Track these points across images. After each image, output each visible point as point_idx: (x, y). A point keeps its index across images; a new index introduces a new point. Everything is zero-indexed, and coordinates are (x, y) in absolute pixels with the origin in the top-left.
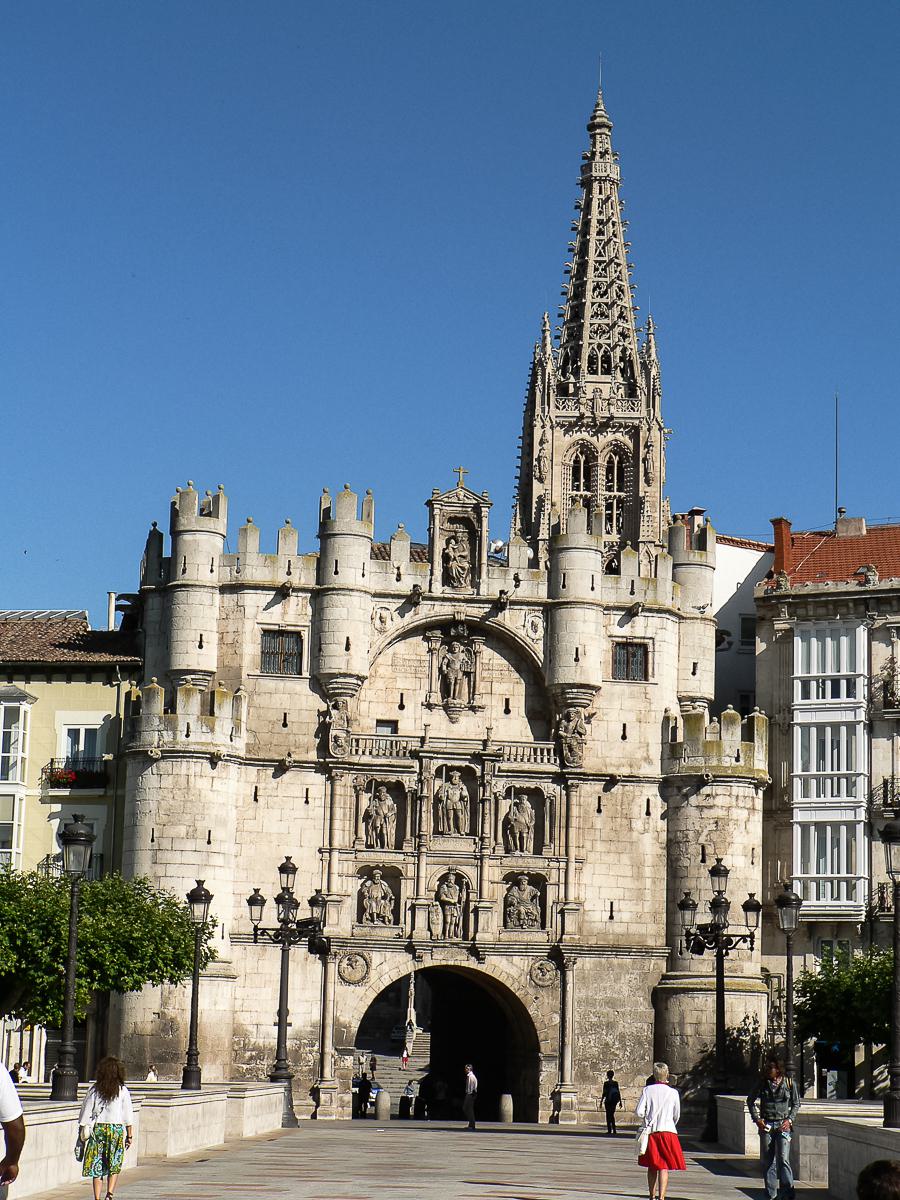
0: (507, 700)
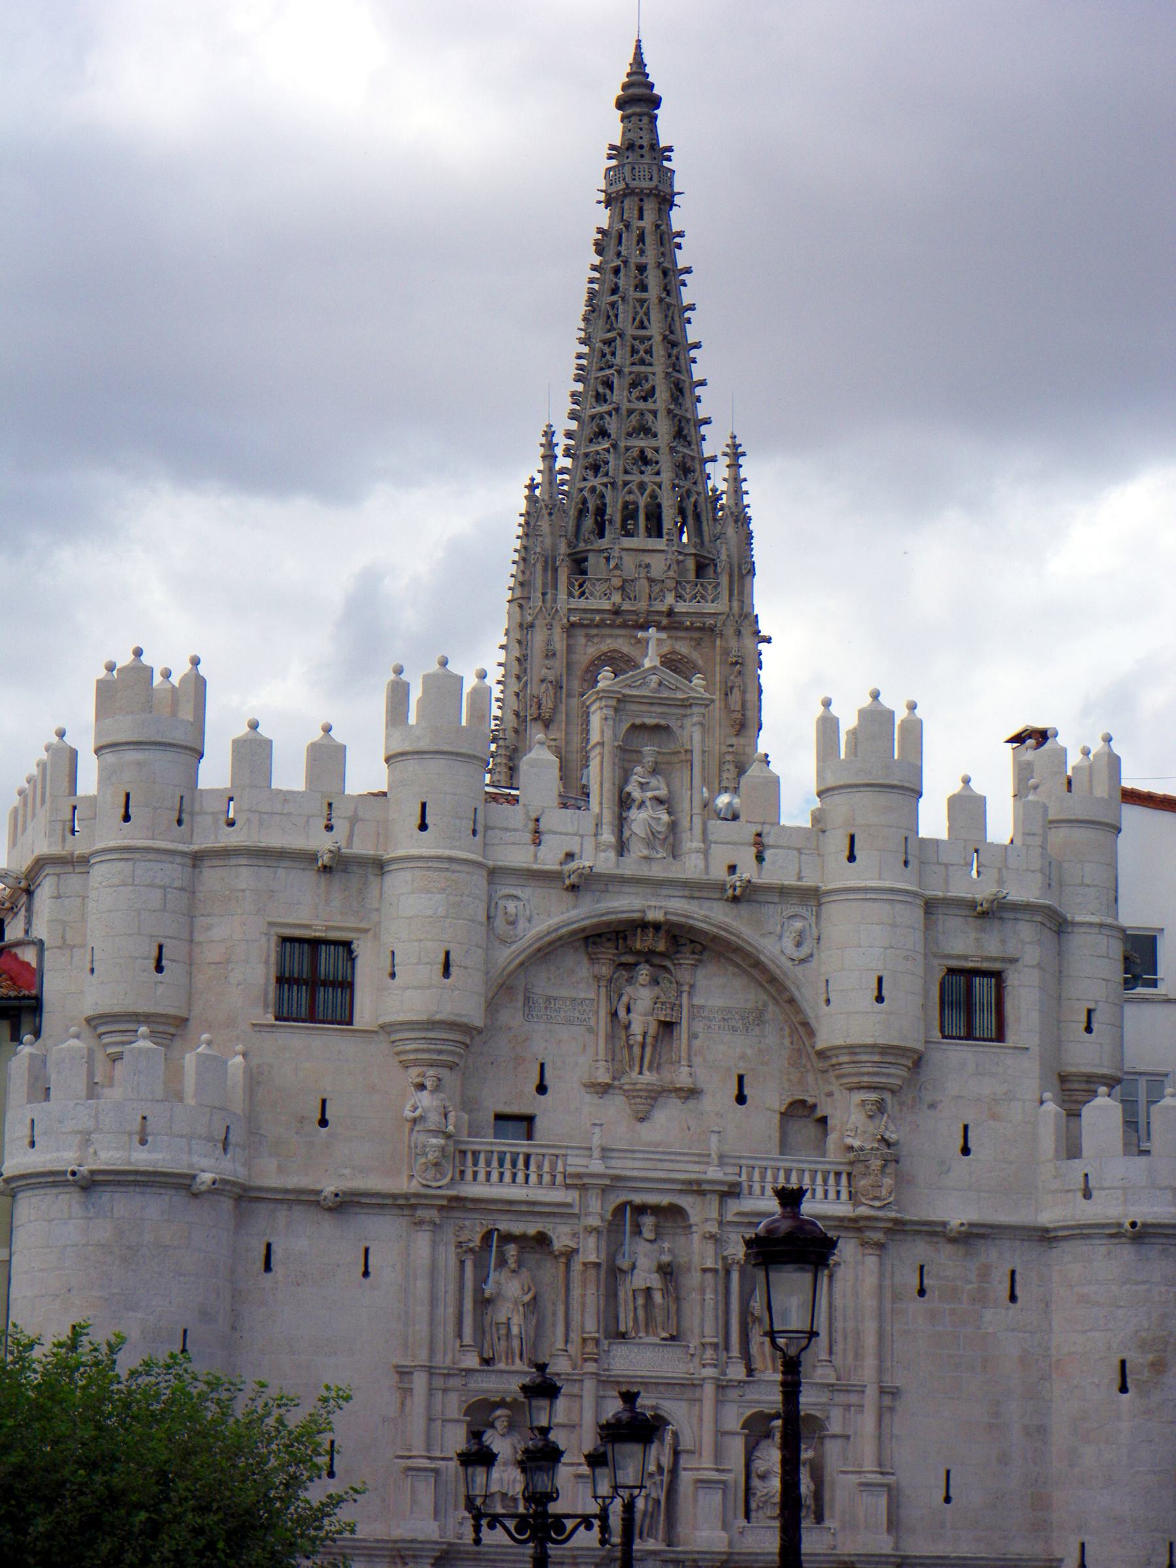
0: (741, 1078)
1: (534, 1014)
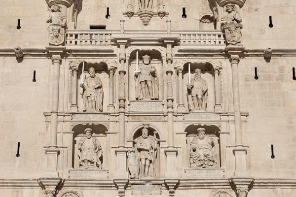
0: (184, 9)
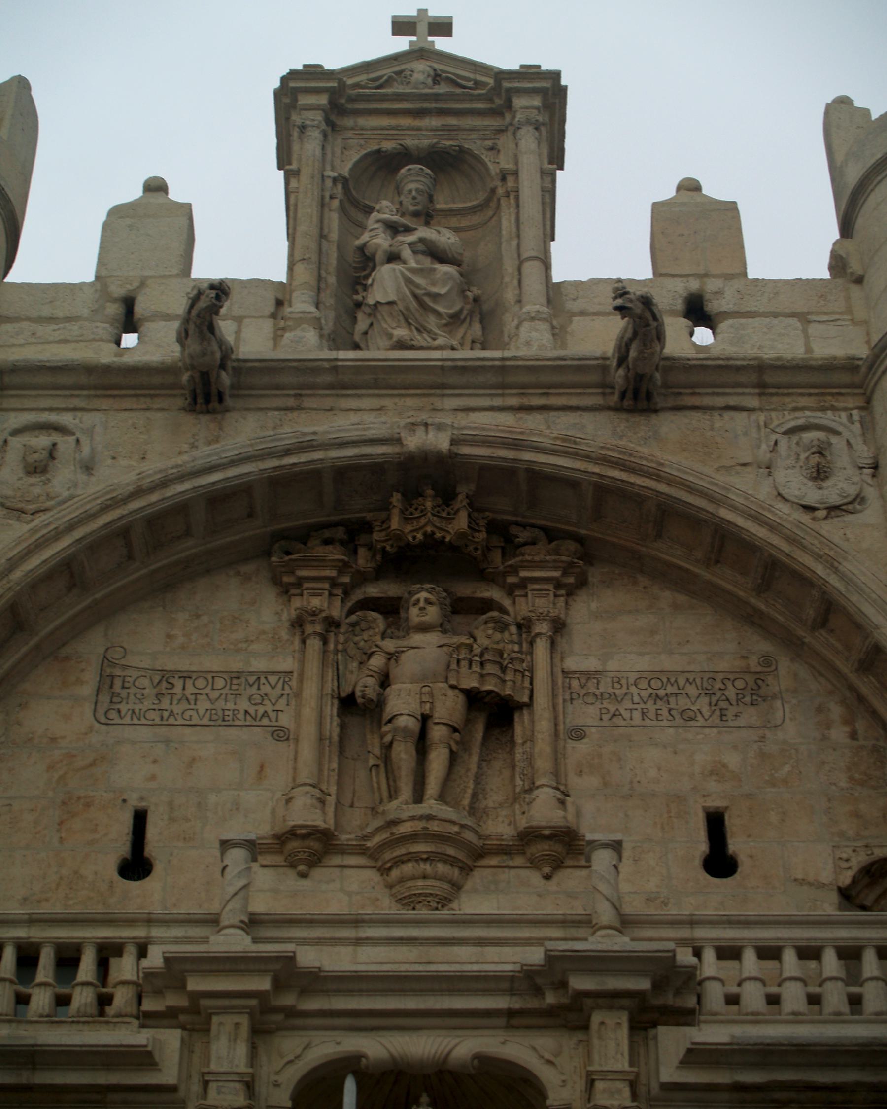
1: (124, 707)
